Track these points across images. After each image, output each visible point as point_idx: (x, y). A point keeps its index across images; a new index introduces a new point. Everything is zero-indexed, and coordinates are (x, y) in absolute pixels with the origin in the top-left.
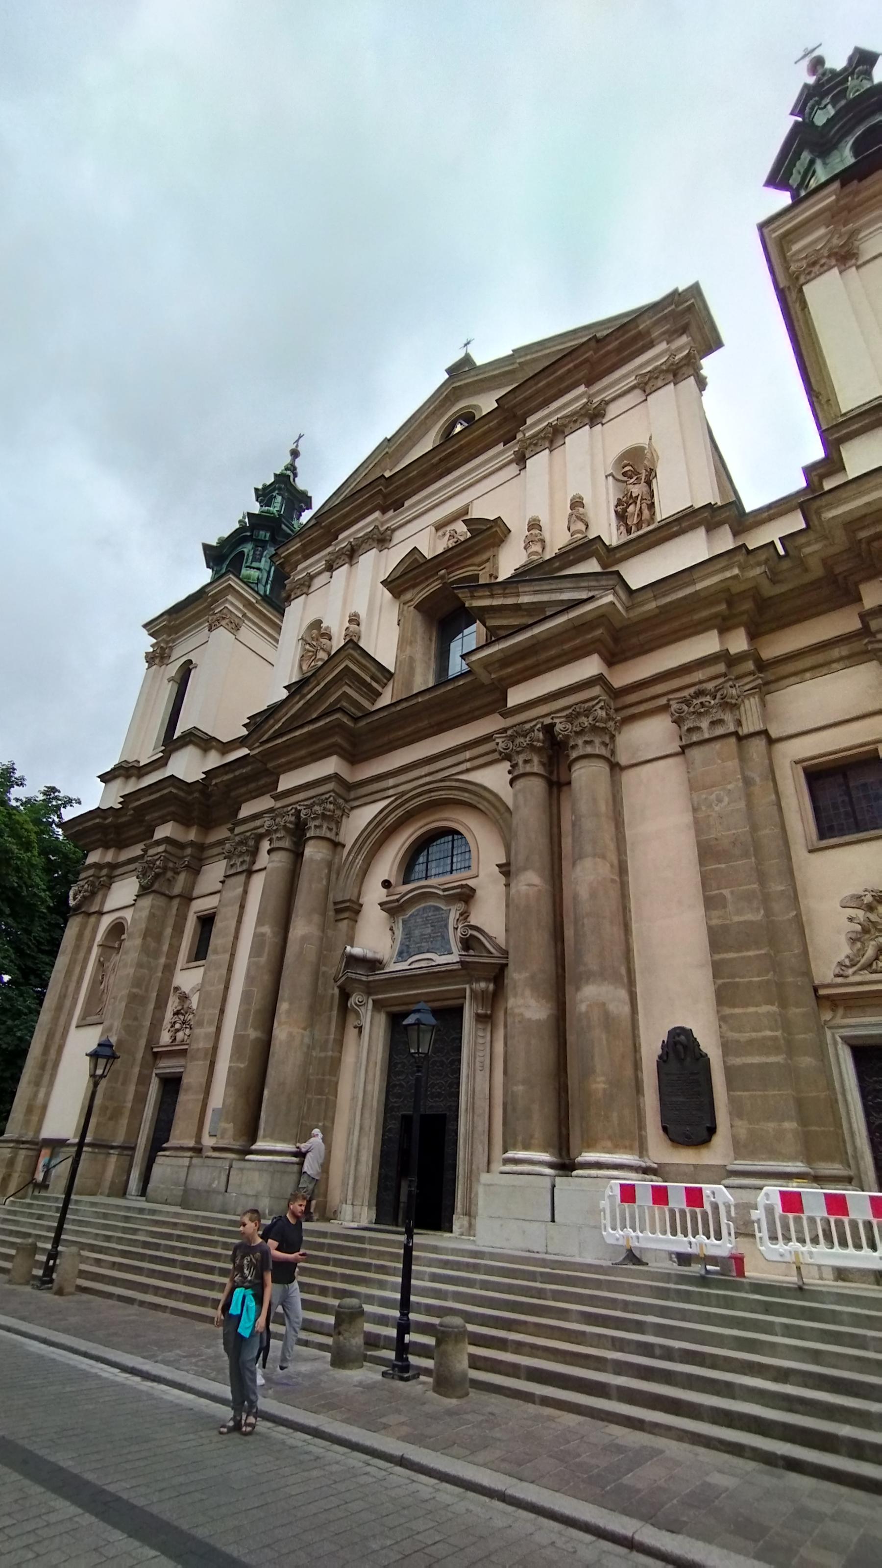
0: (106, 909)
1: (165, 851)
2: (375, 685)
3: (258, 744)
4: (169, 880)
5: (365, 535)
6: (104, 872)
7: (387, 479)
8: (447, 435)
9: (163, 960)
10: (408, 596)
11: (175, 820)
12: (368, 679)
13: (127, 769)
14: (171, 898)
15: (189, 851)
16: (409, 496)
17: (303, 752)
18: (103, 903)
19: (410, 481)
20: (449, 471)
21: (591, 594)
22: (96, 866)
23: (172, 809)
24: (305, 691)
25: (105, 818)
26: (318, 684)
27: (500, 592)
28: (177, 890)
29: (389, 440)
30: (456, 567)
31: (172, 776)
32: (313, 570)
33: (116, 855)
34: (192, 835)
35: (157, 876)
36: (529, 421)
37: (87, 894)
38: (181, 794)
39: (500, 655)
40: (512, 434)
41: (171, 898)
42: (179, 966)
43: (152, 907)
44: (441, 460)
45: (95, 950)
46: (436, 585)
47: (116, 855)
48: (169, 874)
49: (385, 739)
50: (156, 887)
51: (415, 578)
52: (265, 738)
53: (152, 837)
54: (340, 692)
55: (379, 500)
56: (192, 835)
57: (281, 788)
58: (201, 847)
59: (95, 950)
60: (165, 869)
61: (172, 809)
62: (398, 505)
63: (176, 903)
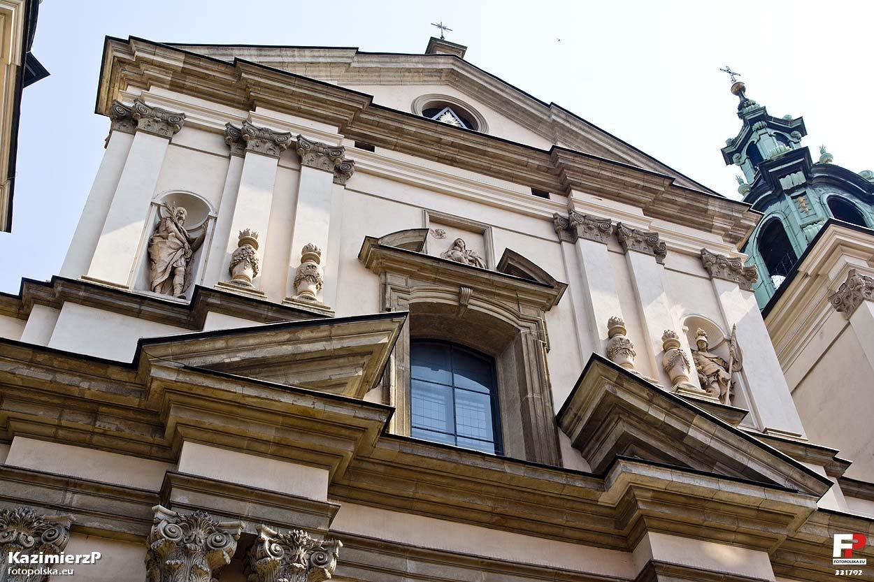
3: (173, 364)
7: (372, 105)
8: (433, 109)
16: (385, 144)
19: (400, 132)
20: (452, 162)
21: (796, 488)
24: (305, 334)
26: (329, 338)
27: (663, 404)
29: (358, 53)
32: (191, 117)
39: (662, 486)
40: (545, 188)
44: (453, 145)
49: (410, 492)
52: (196, 362)
55: (347, 116)
62: (366, 145)
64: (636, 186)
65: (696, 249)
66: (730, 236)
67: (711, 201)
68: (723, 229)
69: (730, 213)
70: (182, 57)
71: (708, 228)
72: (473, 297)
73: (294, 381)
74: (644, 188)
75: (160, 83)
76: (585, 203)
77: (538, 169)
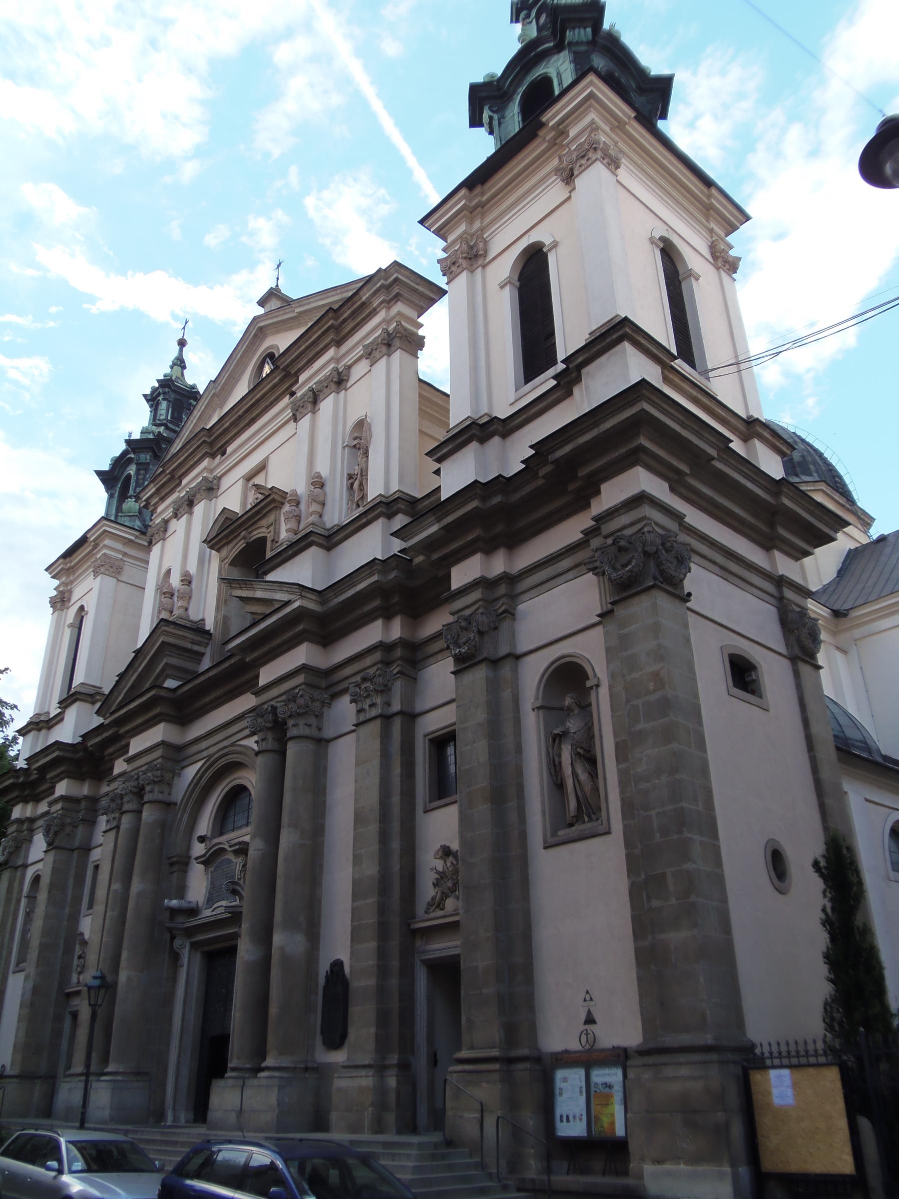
0: (30, 861)
1: (62, 809)
2: (196, 648)
4: (68, 835)
5: (197, 485)
6: (25, 826)
9: (67, 910)
10: (224, 552)
11: (69, 777)
12: (189, 646)
13: (37, 723)
14: (73, 850)
15: (83, 804)
17: (139, 721)
18: (26, 857)
20: (253, 421)
22: (20, 821)
23: (62, 769)
25: (18, 778)
26: (145, 658)
28: (77, 844)
30: (253, 528)
31: (57, 742)
33: (35, 809)
34: (85, 790)
35: (56, 833)
36: (302, 378)
37: (12, 850)
38: (68, 755)
41: (73, 850)
42: (82, 914)
43: (54, 862)
45: (23, 902)
46: (241, 545)
47: (35, 809)
48: (68, 829)
50: (55, 844)
51: (226, 536)
53: (53, 793)
54: (162, 664)
56: (85, 790)
57: (132, 751)
58: (93, 800)
59: (23, 902)
60: (63, 826)
61: (62, 769)
63: (76, 854)
64: (320, 337)
65: (359, 351)
66: (391, 300)
67: (361, 293)
68: (382, 302)
69: (375, 288)
70: (152, 485)
71: (374, 313)
72: (250, 533)
73: (147, 685)
74: (324, 333)
75: (156, 505)
76: (309, 379)
77: (282, 380)
